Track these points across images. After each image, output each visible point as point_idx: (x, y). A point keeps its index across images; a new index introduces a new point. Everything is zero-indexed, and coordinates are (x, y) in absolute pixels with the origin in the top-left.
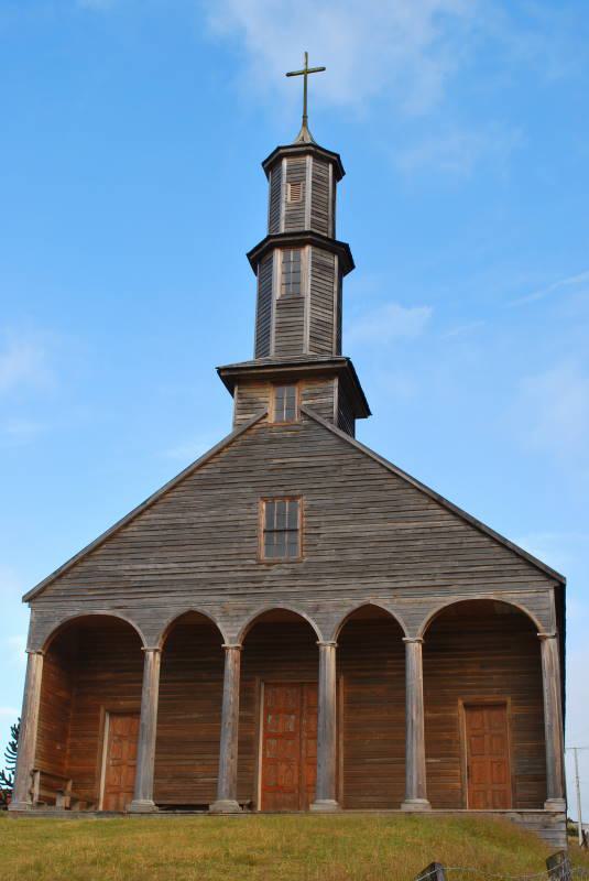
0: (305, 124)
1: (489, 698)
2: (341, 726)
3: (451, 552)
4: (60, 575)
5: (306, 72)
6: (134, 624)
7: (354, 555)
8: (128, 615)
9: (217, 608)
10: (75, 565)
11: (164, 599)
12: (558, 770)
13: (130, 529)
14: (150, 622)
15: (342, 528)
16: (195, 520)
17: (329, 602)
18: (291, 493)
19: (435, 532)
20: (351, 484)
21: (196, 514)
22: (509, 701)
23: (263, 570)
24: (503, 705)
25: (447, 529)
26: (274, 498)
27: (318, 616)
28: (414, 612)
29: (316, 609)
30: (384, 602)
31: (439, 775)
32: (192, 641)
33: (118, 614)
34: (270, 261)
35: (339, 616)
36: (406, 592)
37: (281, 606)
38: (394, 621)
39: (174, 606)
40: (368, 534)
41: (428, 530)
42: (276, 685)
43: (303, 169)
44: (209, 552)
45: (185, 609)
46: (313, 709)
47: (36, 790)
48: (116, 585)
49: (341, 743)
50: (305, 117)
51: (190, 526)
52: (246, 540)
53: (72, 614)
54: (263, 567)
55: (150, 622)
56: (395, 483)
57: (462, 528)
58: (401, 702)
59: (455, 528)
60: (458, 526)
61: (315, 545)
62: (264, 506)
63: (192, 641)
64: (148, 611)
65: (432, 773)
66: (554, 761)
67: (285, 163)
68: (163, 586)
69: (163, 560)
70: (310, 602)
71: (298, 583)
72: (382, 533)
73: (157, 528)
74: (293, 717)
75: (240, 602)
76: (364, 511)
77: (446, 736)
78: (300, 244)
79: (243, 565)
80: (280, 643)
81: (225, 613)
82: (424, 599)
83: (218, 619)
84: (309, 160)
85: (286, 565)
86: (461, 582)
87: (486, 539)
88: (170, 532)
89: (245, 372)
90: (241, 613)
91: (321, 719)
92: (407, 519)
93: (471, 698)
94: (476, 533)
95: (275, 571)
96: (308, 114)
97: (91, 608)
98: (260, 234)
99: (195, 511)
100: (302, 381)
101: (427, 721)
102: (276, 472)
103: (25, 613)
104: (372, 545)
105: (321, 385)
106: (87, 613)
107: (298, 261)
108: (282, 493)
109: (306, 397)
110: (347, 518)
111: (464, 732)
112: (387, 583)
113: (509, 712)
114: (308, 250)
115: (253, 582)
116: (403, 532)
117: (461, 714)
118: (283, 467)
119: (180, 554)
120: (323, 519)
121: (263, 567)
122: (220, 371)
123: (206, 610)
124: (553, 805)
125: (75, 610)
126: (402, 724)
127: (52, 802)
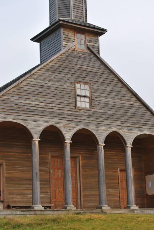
2: (81, 175)
3: (139, 115)
8: (25, 123)
9: (62, 125)
13: (22, 84)
14: (36, 127)
15: (104, 99)
16: (50, 85)
20: (106, 82)
21: (50, 83)
23: (78, 112)
25: (137, 106)
27: (98, 133)
28: (129, 137)
30: (120, 131)
33: (21, 122)
37: (85, 128)
40: (113, 103)
41: (131, 106)
44: (55, 100)
45: (48, 124)
48: (17, 109)
49: (81, 182)
52: (71, 98)
54: (78, 110)
55: (36, 127)
56: (120, 85)
57: (142, 107)
59: (140, 106)
61: (96, 105)
63: (52, 137)
69: (39, 101)
70: (95, 128)
71: (91, 119)
72: (117, 104)
73: (35, 86)
74: (60, 171)
75: (70, 124)
76: (111, 94)
79: (70, 109)
81: (65, 127)
82: (132, 131)
83: (62, 130)
85: (86, 111)
86: (142, 127)
87: (149, 112)
88: (40, 89)
89: (69, 24)
90: (71, 129)
92: (125, 100)
94: (145, 109)
95: (82, 113)
97: (8, 118)
99: (50, 81)
102: (80, 71)
104: (114, 108)
105: (93, 38)
106: (7, 120)
108: (82, 80)
110: (105, 95)
112: (119, 123)
115: (74, 116)
116: (124, 105)
118: (81, 69)
119: (45, 99)
120: (98, 94)
121: (78, 110)
123: (57, 125)
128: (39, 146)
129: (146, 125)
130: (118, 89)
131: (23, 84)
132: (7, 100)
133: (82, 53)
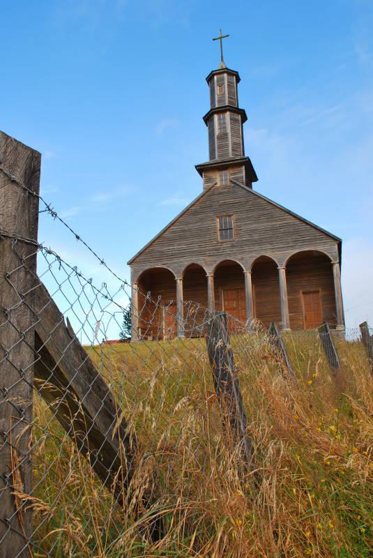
0: (222, 60)
1: (312, 290)
4: (140, 254)
5: (221, 38)
6: (171, 270)
7: (256, 237)
8: (169, 267)
10: (146, 249)
11: (182, 260)
12: (341, 315)
14: (177, 269)
15: (250, 227)
17: (246, 256)
18: (230, 214)
19: (288, 225)
22: (320, 290)
24: (318, 292)
26: (222, 217)
28: (281, 258)
29: (242, 259)
30: (269, 254)
31: (294, 320)
32: (194, 276)
33: (164, 267)
34: (213, 120)
35: (251, 261)
36: (278, 250)
38: (273, 262)
39: (186, 262)
42: (227, 290)
43: (223, 79)
45: (191, 262)
46: (243, 298)
47: (140, 334)
48: (162, 256)
50: (222, 57)
51: (190, 230)
53: (147, 268)
55: (177, 269)
56: (269, 207)
58: (278, 293)
60: (297, 222)
62: (218, 220)
63: (194, 276)
64: (176, 265)
65: (291, 319)
66: (340, 312)
67: (215, 77)
68: (182, 254)
69: (180, 244)
70: (240, 256)
77: (296, 305)
78: (225, 111)
80: (229, 274)
81: (206, 263)
84: (225, 75)
91: (247, 301)
92: (276, 221)
93: (305, 290)
95: (224, 245)
96: (223, 55)
98: (207, 109)
100: (230, 167)
101: (289, 300)
103: (129, 268)
107: (224, 118)
109: (232, 174)
111: (303, 303)
113: (320, 294)
114: (228, 113)
117: (301, 295)
118: (225, 204)
122: (196, 167)
123: (199, 263)
124: (339, 328)
125: (147, 267)
126: (279, 301)
127: (146, 339)
128: (252, 280)
129: (304, 241)
130: (266, 212)
131: (167, 234)
132: (153, 251)
133: (225, 187)
